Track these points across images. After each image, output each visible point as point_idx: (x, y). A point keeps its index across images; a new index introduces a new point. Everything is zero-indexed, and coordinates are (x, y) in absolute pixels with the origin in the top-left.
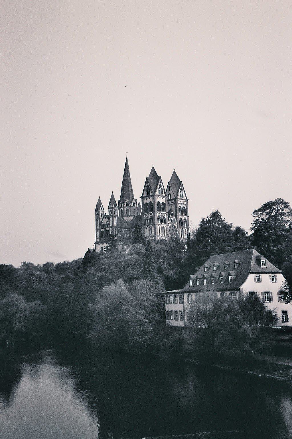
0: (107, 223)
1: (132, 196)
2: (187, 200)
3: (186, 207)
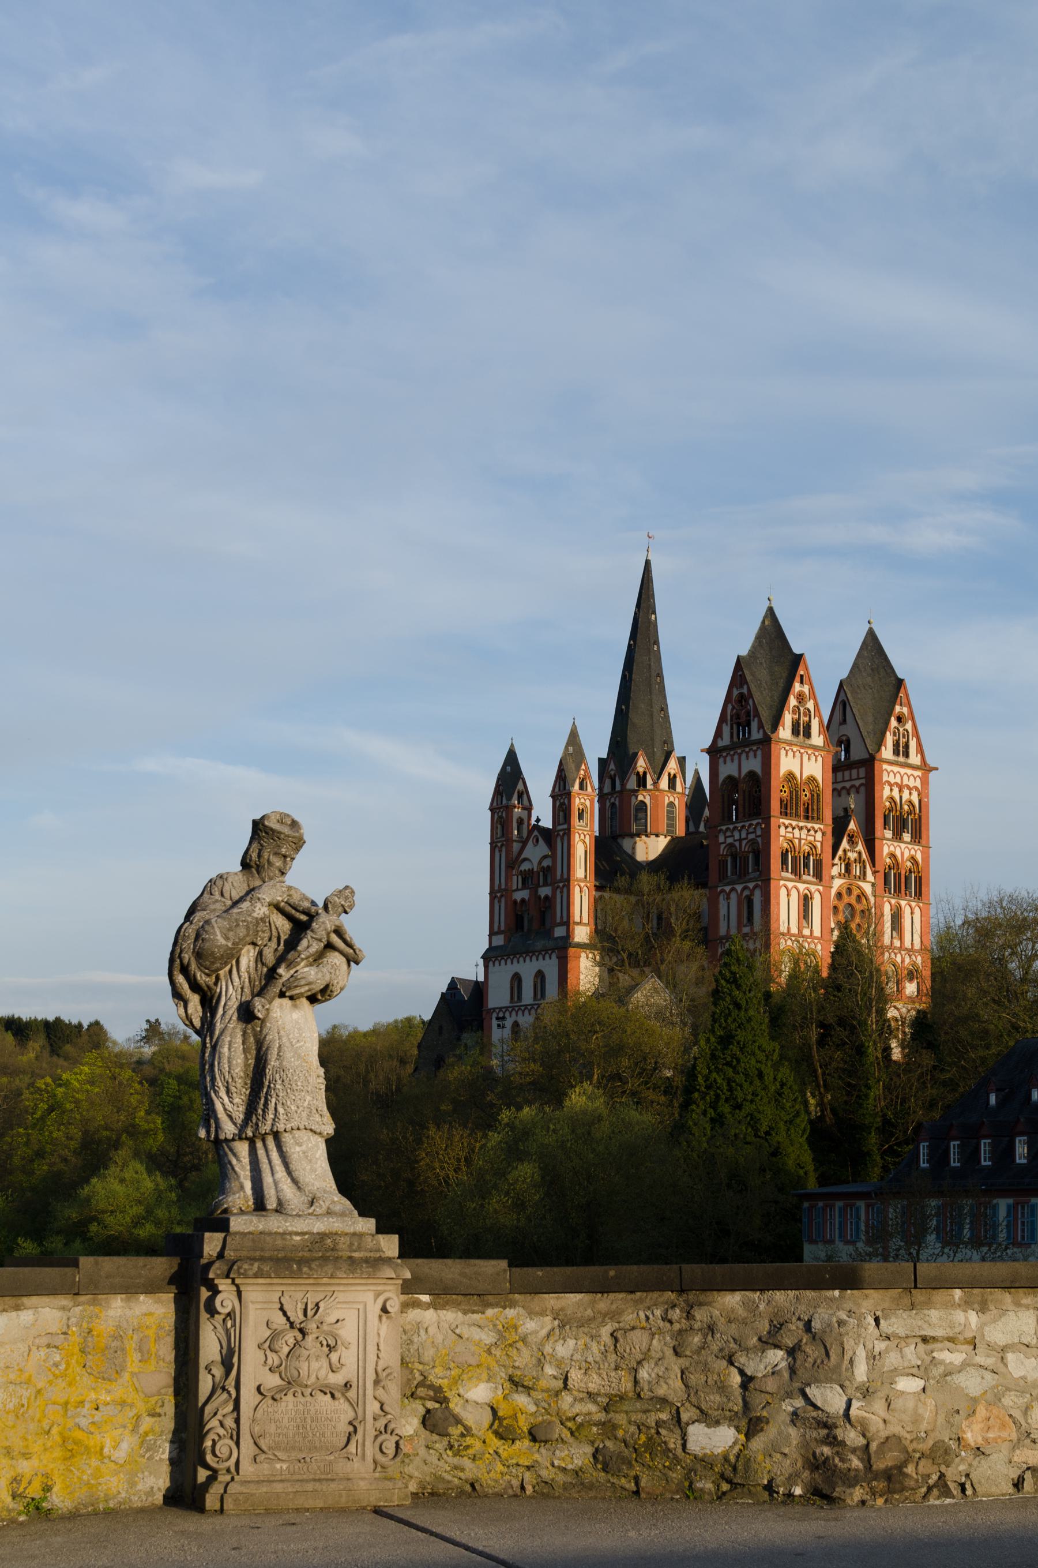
0: (546, 863)
3: (920, 801)
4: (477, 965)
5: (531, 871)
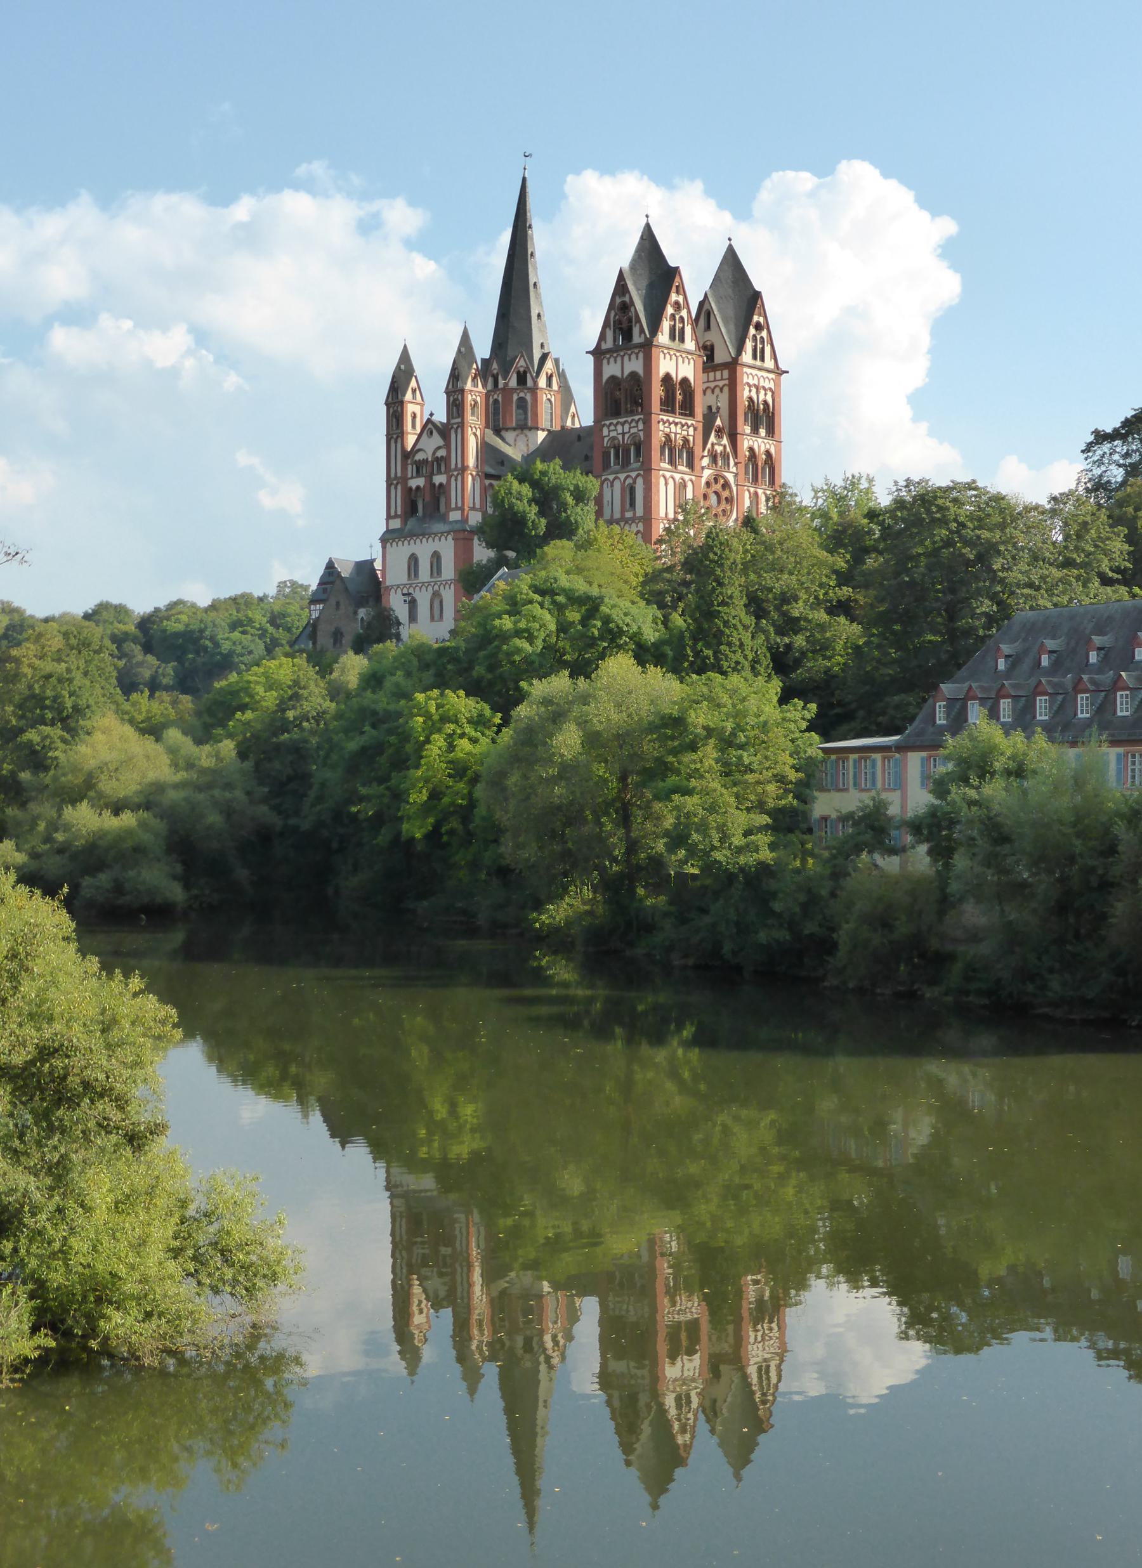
0: (440, 453)
1: (542, 346)
3: (773, 400)
4: (371, 546)
5: (425, 461)
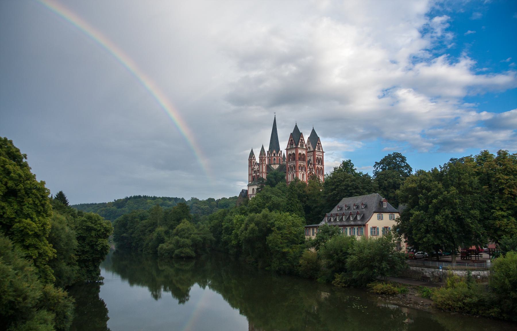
0: (258, 169)
2: (323, 152)
